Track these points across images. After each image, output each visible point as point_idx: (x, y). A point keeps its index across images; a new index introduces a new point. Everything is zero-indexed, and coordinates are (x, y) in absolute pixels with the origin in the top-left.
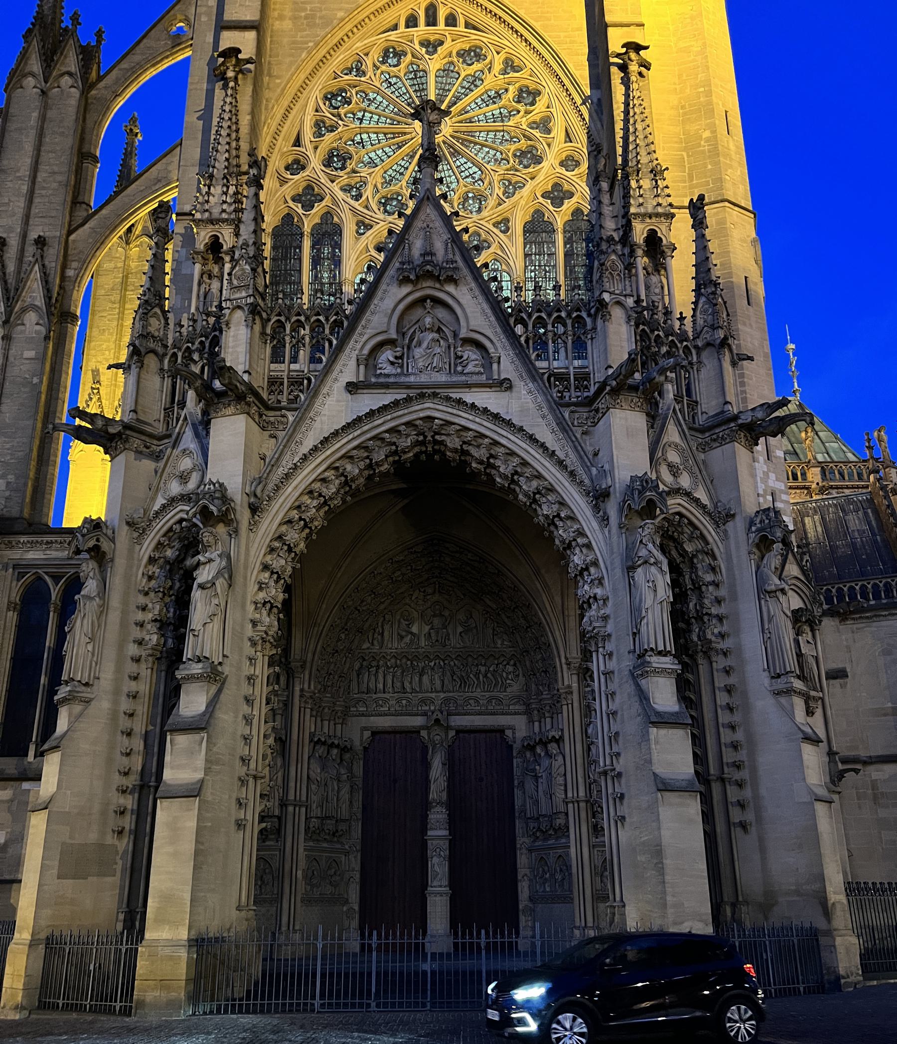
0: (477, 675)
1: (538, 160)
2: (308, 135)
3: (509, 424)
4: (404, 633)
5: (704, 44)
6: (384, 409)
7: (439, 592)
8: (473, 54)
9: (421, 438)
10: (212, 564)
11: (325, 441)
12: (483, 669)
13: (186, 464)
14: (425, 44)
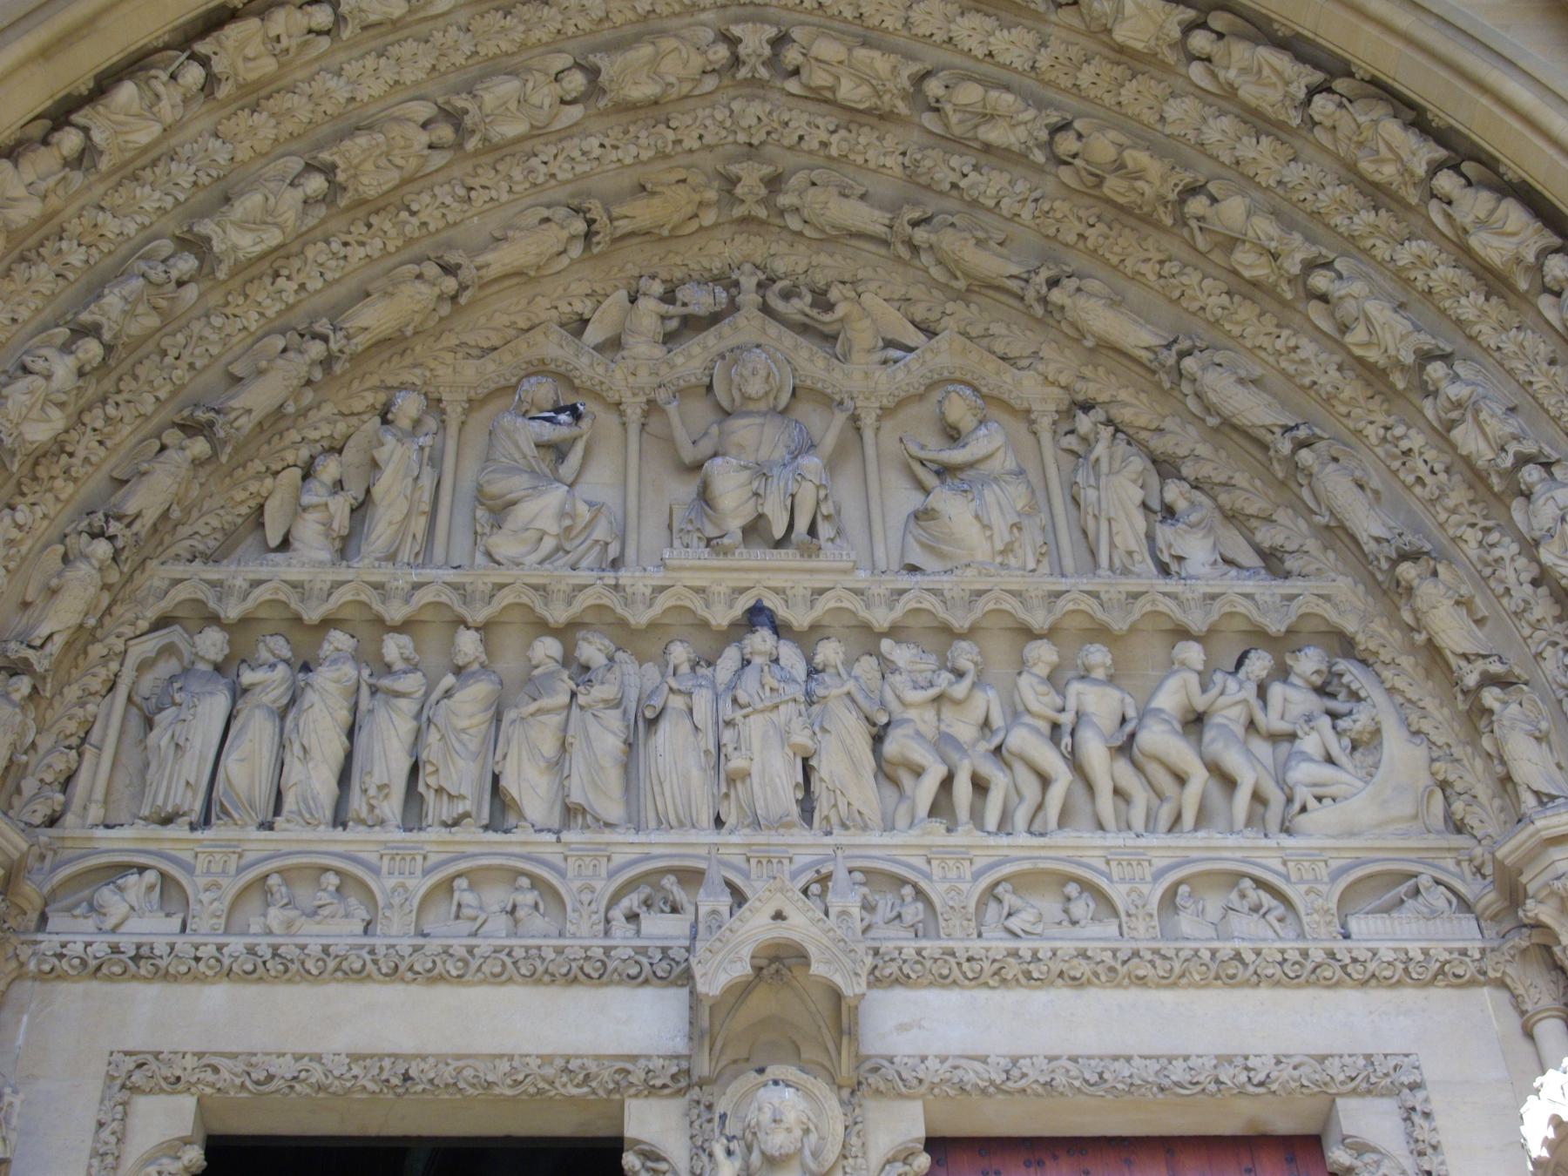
4: (516, 484)
7: (766, 309)
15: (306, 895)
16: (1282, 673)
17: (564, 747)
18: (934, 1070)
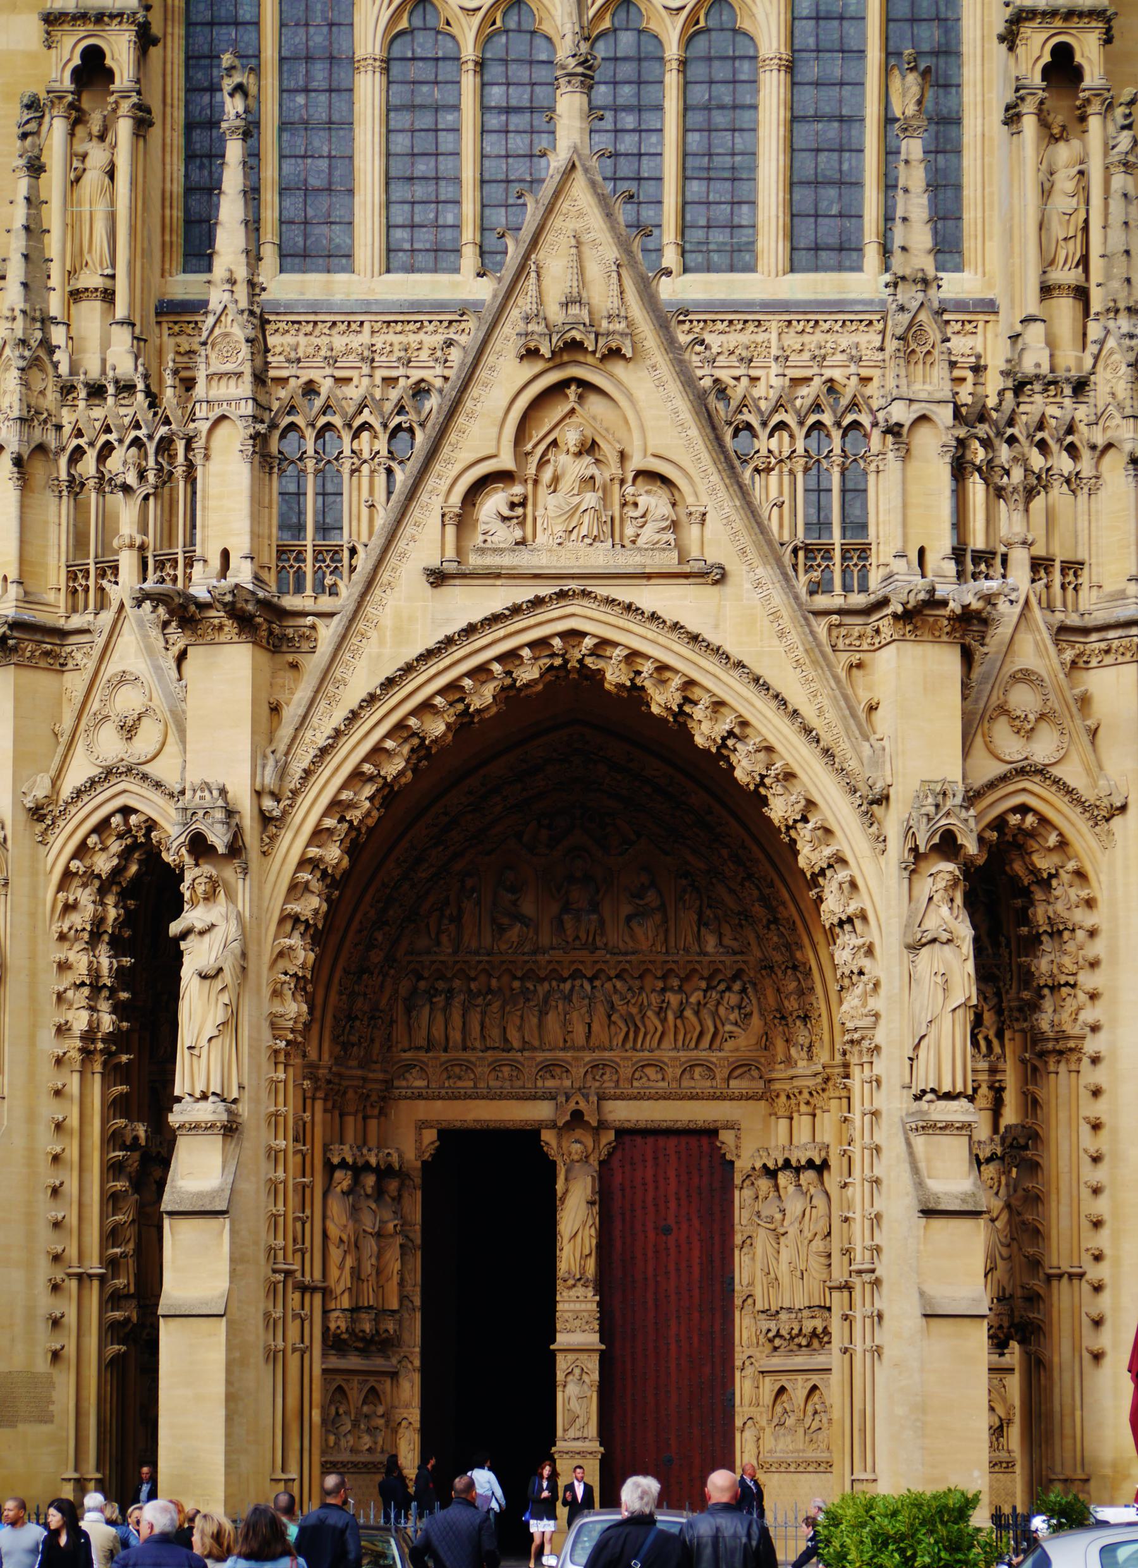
0: (661, 1012)
3: (717, 651)
4: (505, 921)
6: (494, 619)
9: (558, 662)
10: (216, 930)
11: (389, 683)
12: (674, 999)
13: (128, 701)
15: (457, 1070)
16: (729, 989)
17: (522, 1018)
18: (617, 1124)
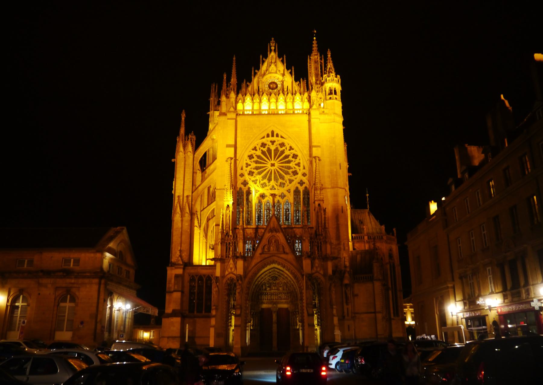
1: (297, 174)
2: (244, 168)
5: (336, 146)
8: (282, 145)
11: (256, 265)
12: (284, 295)
14: (271, 142)
